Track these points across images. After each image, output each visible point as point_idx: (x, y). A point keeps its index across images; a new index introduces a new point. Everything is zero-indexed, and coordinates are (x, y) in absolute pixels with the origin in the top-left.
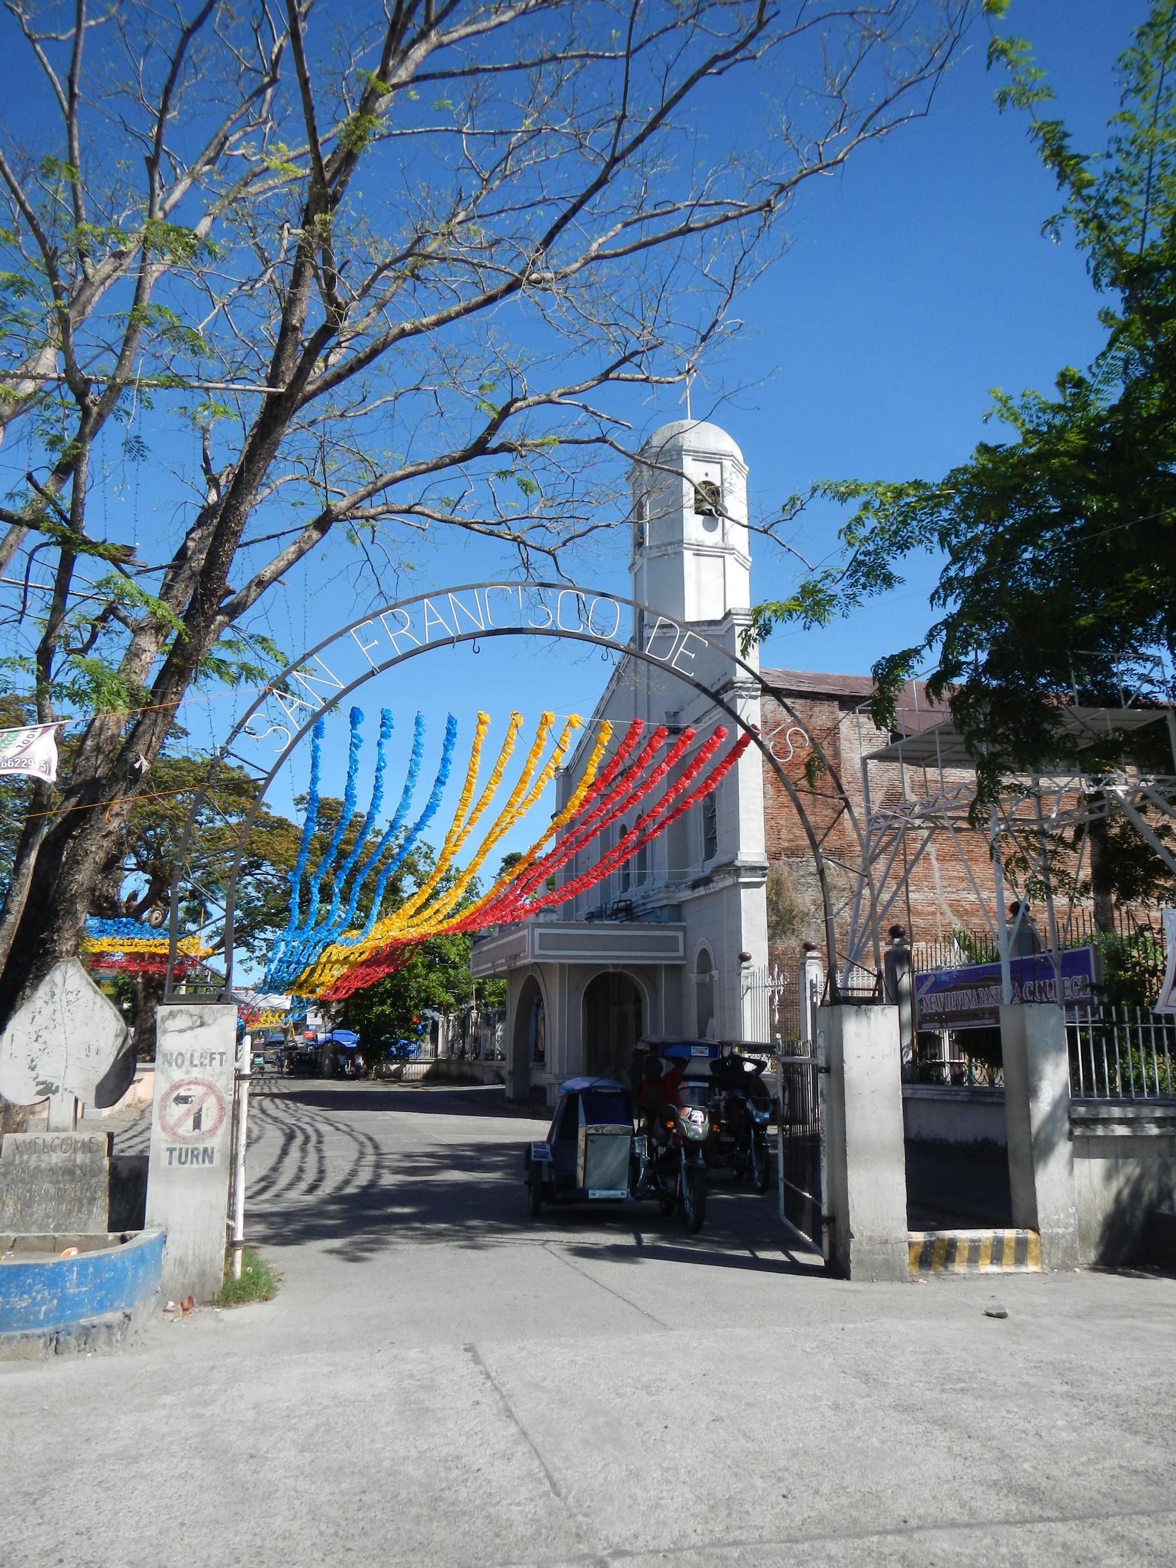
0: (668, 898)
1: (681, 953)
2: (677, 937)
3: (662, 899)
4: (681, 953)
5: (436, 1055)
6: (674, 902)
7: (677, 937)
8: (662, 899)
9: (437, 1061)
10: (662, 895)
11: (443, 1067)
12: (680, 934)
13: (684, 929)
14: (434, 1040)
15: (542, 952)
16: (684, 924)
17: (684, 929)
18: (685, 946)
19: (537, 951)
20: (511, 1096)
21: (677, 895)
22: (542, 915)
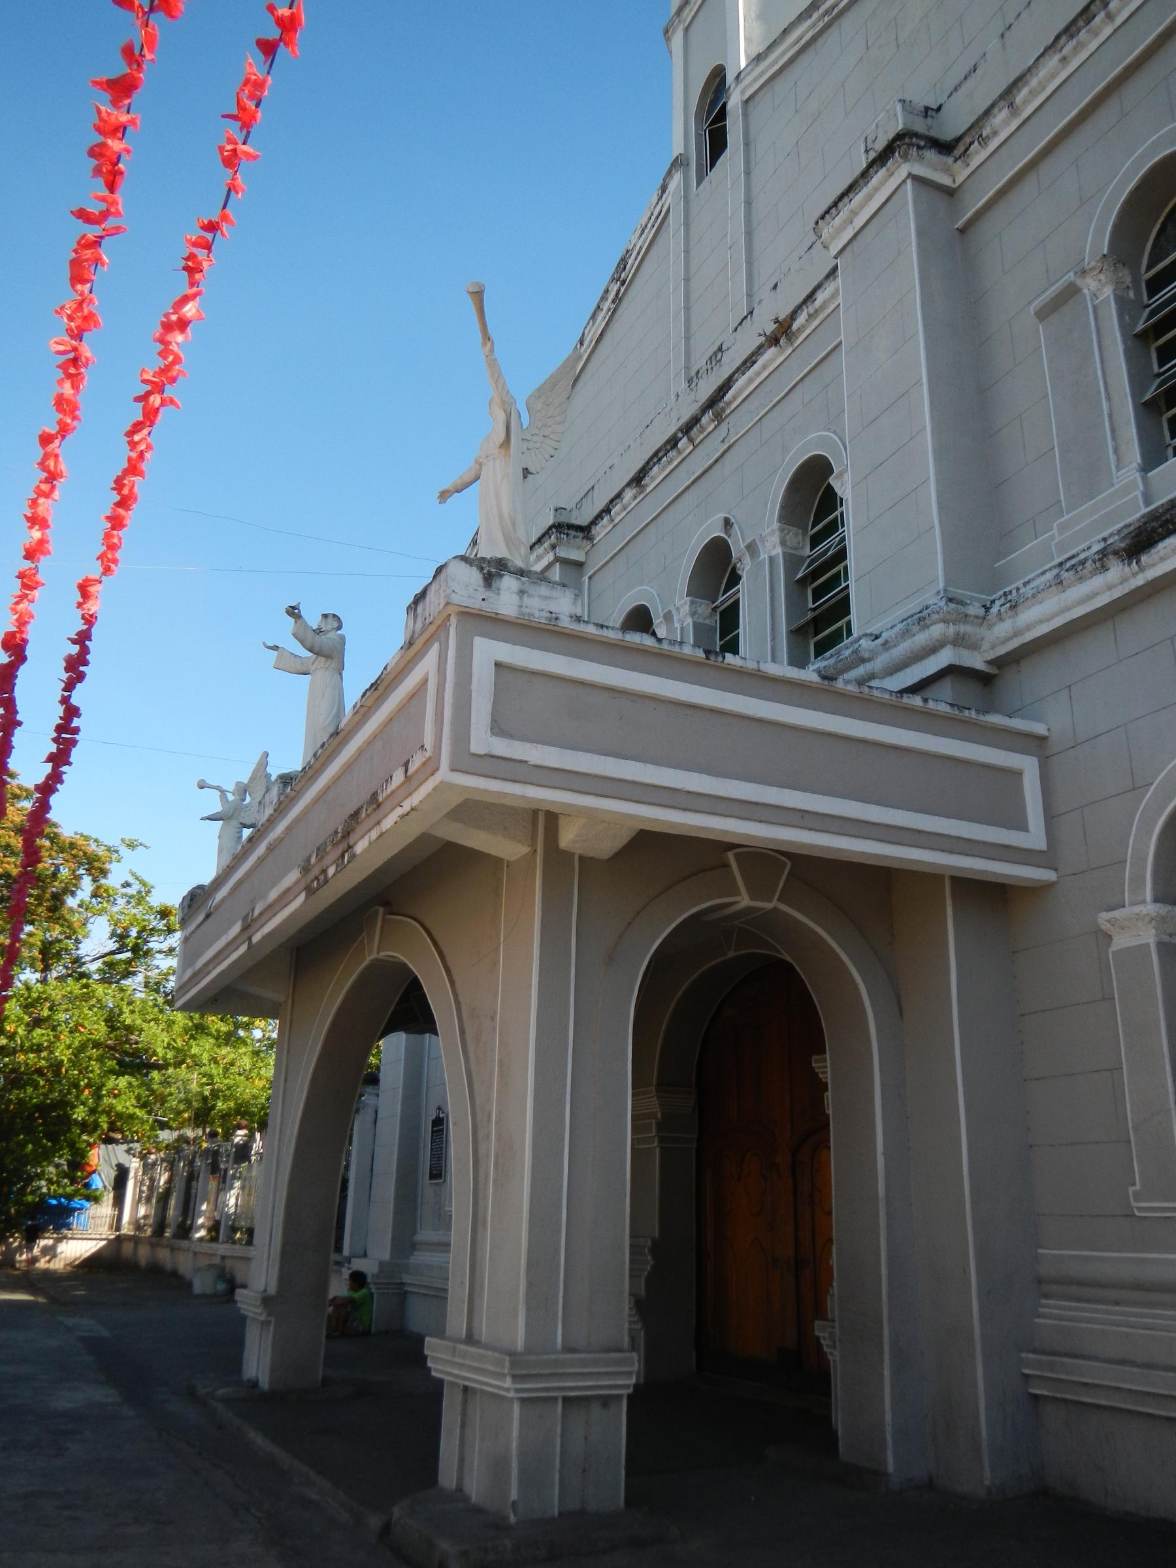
0: (959, 641)
1: (1035, 837)
2: (1018, 774)
3: (932, 650)
4: (1035, 837)
5: (118, 1229)
6: (977, 661)
7: (1018, 774)
8: (932, 650)
9: (118, 1237)
10: (937, 631)
11: (128, 1249)
12: (1028, 765)
13: (1036, 744)
14: (119, 1202)
15: (502, 747)
16: (1039, 729)
17: (1036, 744)
18: (1050, 817)
19: (482, 740)
20: (265, 1383)
21: (1003, 629)
22: (509, 583)
